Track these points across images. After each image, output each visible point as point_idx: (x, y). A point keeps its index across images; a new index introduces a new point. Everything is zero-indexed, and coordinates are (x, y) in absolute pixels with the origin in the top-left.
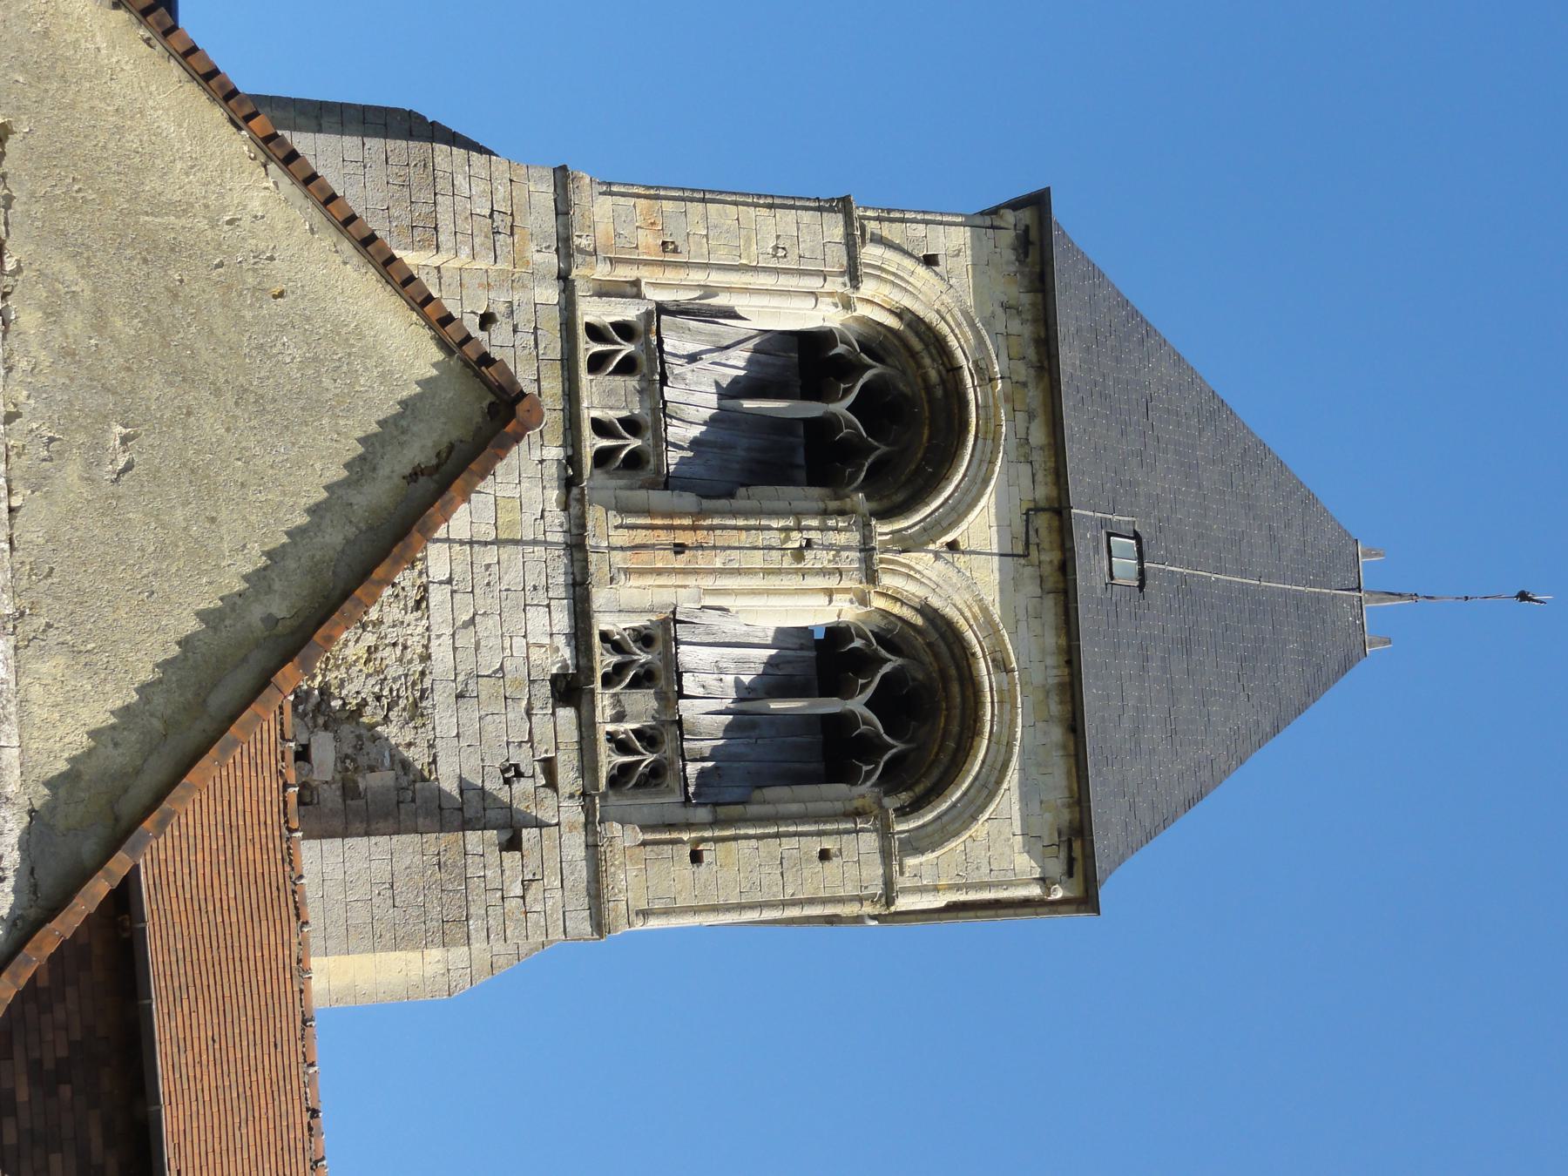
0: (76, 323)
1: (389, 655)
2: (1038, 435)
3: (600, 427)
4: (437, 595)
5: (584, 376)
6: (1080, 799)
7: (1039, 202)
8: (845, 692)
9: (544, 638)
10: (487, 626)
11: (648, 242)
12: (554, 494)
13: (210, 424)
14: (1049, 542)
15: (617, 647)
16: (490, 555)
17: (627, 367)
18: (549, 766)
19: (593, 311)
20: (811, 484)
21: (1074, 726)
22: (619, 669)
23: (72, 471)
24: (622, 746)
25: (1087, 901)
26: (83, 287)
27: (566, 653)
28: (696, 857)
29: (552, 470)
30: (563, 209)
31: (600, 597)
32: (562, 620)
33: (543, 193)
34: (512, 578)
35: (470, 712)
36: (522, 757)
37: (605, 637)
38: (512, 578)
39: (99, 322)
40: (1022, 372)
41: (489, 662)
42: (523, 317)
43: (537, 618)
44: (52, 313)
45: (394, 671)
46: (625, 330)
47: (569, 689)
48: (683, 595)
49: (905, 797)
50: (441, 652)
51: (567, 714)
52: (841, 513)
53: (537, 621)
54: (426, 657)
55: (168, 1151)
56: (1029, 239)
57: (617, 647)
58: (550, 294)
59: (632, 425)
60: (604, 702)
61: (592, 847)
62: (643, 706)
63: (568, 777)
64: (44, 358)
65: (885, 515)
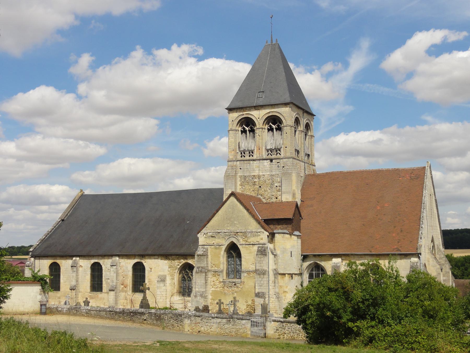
2: (248, 109)
3: (250, 156)
6: (282, 104)
7: (226, 109)
8: (273, 128)
9: (267, 163)
10: (266, 169)
11: (233, 152)
14: (257, 107)
17: (244, 153)
19: (239, 157)
21: (275, 105)
30: (231, 161)
31: (264, 157)
32: (265, 161)
33: (230, 163)
39: (229, 223)
40: (242, 110)
43: (265, 164)
44: (228, 227)
45: (270, 178)
46: (241, 153)
47: (271, 160)
48: (264, 148)
50: (268, 173)
53: (265, 164)
56: (230, 110)
58: (238, 162)
59: (250, 153)
60: (274, 156)
63: (278, 161)
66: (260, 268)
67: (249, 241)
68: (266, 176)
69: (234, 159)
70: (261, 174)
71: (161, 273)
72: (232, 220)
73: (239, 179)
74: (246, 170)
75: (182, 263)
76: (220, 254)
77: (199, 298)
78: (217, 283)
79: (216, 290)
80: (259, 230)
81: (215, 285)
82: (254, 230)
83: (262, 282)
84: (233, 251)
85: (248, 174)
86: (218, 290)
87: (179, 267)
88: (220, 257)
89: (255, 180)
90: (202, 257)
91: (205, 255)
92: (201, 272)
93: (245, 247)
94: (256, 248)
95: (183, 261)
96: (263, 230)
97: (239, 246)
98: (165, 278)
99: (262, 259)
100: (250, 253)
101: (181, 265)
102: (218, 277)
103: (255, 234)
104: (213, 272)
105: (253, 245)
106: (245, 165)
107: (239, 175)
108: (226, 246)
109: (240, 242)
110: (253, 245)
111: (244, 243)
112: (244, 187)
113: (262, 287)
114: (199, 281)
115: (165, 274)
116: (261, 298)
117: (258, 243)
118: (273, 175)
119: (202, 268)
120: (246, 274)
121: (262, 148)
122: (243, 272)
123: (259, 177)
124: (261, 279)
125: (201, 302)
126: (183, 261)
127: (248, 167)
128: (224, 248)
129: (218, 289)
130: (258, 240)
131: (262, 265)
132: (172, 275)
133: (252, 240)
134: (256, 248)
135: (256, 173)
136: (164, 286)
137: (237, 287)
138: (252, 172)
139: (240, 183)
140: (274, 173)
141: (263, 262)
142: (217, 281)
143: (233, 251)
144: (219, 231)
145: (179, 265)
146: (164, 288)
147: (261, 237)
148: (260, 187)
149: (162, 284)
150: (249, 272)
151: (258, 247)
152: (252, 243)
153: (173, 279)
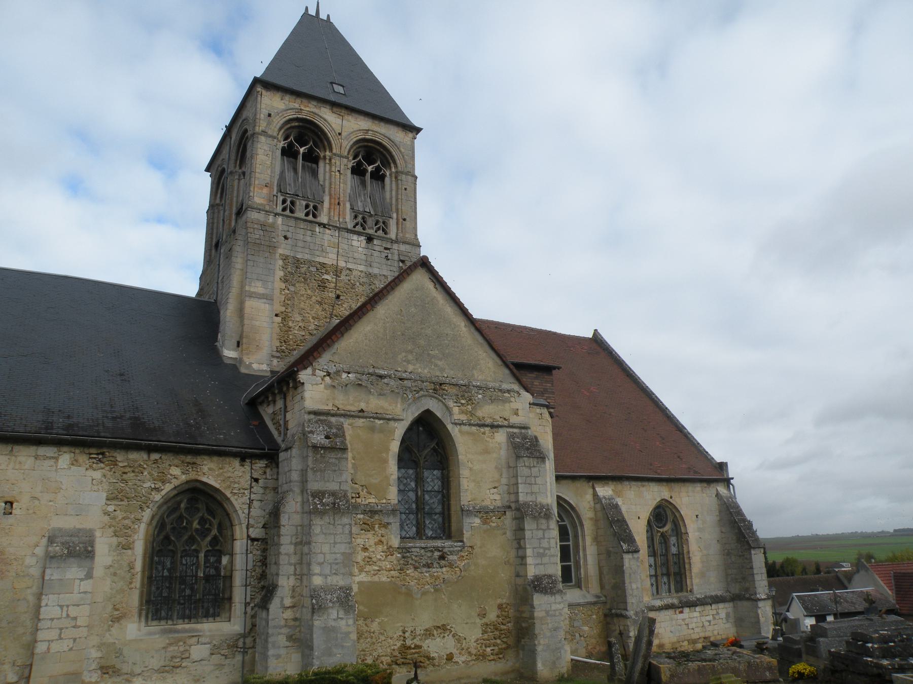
0: (410, 357)
1: (362, 280)
3: (307, 214)
4: (350, 266)
5: (295, 215)
9: (359, 242)
11: (265, 191)
12: (327, 231)
13: (429, 332)
15: (357, 224)
16: (341, 251)
18: (386, 249)
19: (279, 208)
20: (317, 163)
22: (362, 225)
23: (439, 363)
24: (379, 229)
25: (418, 130)
26: (404, 354)
27: (363, 238)
28: (404, 220)
29: (322, 229)
34: (346, 247)
35: (374, 264)
36: (384, 255)
37: (354, 227)
38: (346, 247)
39: (411, 352)
41: (364, 257)
42: (286, 228)
43: (355, 243)
44: (408, 362)
45: (364, 280)
46: (284, 202)
47: (370, 239)
49: (392, 165)
50: (362, 268)
51: (375, 242)
52: (330, 160)
54: (361, 271)
55: (537, 363)
57: (357, 224)
60: (371, 232)
61: (404, 243)
62: (370, 222)
64: (418, 365)
65: (331, 150)
66: (529, 498)
67: (480, 413)
68: (355, 273)
69: (267, 208)
70: (342, 264)
71: (69, 523)
72: (422, 342)
73: (280, 262)
74: (300, 244)
75: (176, 482)
76: (387, 450)
77: (334, 613)
78: (378, 553)
79: (376, 579)
80: (505, 386)
81: (369, 561)
82: (491, 385)
83: (545, 544)
84: (427, 445)
85: (307, 257)
86: (384, 579)
87: (157, 497)
88: (386, 461)
89: (326, 277)
90: (332, 457)
91: (336, 446)
92: (335, 509)
93: (469, 433)
94: (501, 437)
95: (177, 474)
96: (516, 387)
97: (450, 427)
98: (92, 543)
99: (535, 471)
100: (486, 451)
101: (168, 487)
102: (383, 531)
103: (497, 395)
104: (364, 512)
105: (492, 426)
106: (301, 234)
107: (280, 251)
108: (406, 424)
109: (452, 415)
110: (492, 426)
111: (464, 418)
112: (292, 289)
113: (545, 560)
114: (326, 548)
115: (87, 525)
116: (552, 594)
117: (506, 423)
118: (376, 275)
119: (333, 494)
120: (477, 521)
121: (344, 204)
122: (469, 513)
123: (337, 272)
124: (540, 533)
125: (344, 629)
126: (177, 474)
127: (308, 239)
128: (400, 430)
129: (384, 578)
130: (506, 415)
131: (535, 489)
132: (122, 534)
133: (488, 411)
134: (501, 437)
135: (330, 259)
136: (89, 576)
137: (451, 566)
138: (317, 253)
139: (282, 274)
140: (376, 271)
141: (539, 480)
142: (380, 548)
143: (427, 445)
144: (382, 372)
145: (157, 490)
146: (87, 585)
147: (514, 405)
148: (338, 297)
149: (74, 572)
150: (485, 513)
151: (511, 436)
152: (488, 421)
153: (128, 547)
